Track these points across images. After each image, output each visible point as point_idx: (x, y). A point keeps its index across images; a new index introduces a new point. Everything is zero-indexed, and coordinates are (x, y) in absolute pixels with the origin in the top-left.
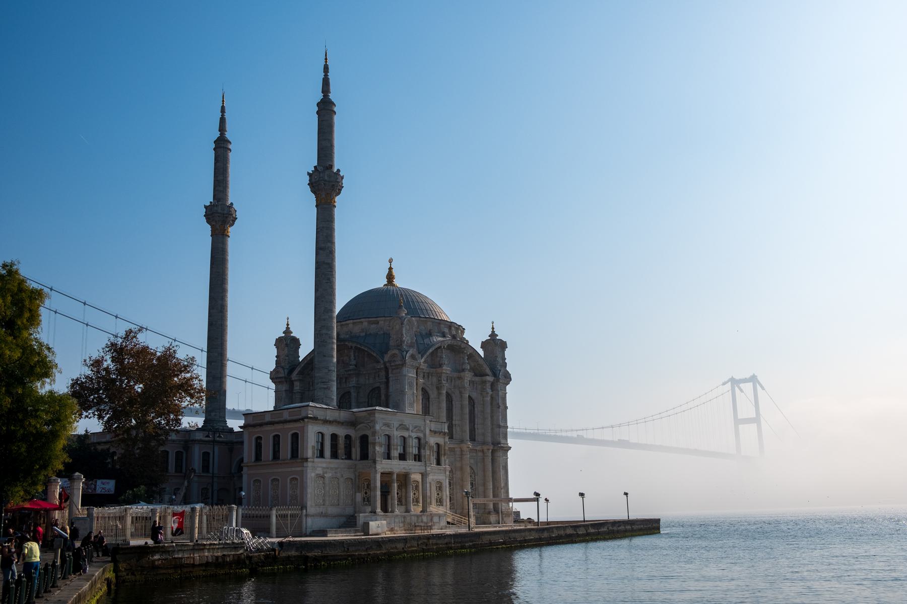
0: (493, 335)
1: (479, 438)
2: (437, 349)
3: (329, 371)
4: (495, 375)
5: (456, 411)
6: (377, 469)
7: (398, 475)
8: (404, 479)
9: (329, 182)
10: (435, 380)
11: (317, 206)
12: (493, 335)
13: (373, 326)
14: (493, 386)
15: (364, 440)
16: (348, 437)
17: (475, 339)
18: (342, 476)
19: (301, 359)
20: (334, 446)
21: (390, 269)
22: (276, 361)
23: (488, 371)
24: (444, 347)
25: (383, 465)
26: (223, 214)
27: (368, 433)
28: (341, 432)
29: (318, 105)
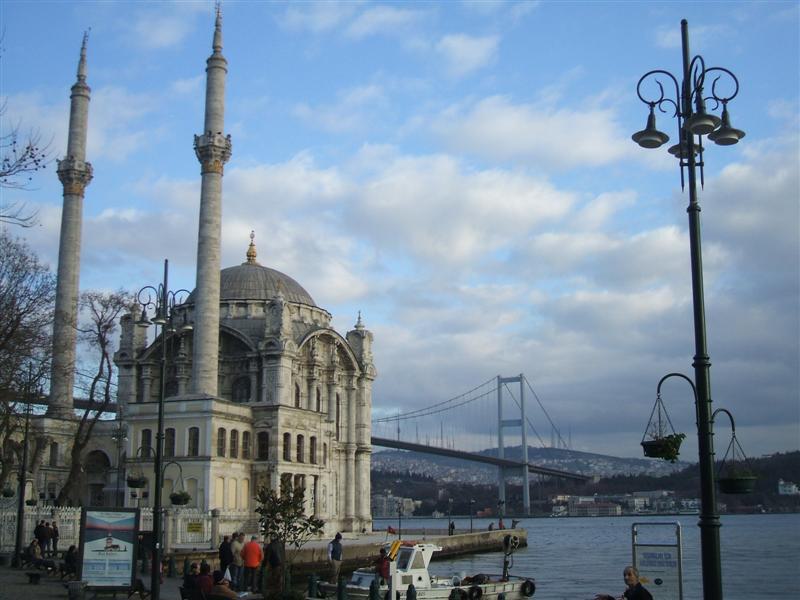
1: (343, 439)
4: (361, 368)
11: (202, 174)
13: (242, 309)
14: (359, 379)
20: (234, 443)
21: (252, 245)
25: (283, 468)
26: (80, 172)
27: (268, 430)
28: (242, 428)
29: (208, 62)
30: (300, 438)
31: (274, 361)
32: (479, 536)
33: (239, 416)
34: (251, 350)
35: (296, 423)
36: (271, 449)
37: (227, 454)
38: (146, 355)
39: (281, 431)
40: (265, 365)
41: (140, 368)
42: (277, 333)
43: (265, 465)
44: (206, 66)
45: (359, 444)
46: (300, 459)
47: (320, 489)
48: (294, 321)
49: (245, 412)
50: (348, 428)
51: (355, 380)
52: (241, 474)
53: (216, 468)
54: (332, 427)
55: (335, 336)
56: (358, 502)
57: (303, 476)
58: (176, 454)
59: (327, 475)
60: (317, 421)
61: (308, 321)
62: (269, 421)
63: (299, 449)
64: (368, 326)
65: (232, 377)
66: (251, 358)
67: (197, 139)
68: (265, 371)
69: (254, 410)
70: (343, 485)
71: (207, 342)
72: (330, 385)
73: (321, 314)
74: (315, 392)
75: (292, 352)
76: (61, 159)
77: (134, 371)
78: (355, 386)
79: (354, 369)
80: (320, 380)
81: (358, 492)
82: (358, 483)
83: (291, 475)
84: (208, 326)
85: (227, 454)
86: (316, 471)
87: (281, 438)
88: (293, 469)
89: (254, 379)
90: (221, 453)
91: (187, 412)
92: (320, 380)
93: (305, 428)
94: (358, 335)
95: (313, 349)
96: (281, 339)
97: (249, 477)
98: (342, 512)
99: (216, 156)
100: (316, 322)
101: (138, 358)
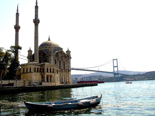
0: (68, 50)
1: (65, 69)
4: (68, 57)
5: (61, 64)
8: (51, 76)
10: (57, 58)
12: (68, 50)
15: (43, 69)
16: (40, 68)
17: (65, 50)
23: (67, 56)
25: (47, 74)
28: (39, 67)
30: (50, 69)
64: (70, 50)
77: (30, 59)
87: (46, 69)
88: (49, 74)
94: (68, 52)
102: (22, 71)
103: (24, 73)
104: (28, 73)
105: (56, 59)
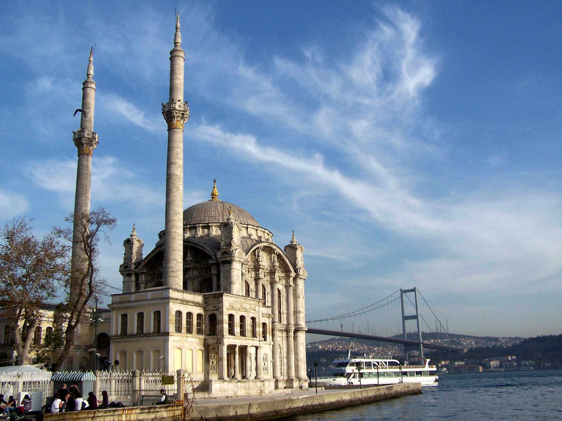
2: (255, 250)
3: (178, 262)
4: (296, 271)
5: (268, 298)
6: (224, 343)
7: (239, 346)
8: (243, 350)
9: (180, 111)
13: (206, 230)
14: (295, 279)
16: (199, 316)
18: (195, 348)
19: (144, 257)
20: (189, 323)
22: (124, 258)
24: (261, 248)
25: (228, 340)
26: (89, 138)
27: (216, 312)
30: (242, 318)
31: (228, 265)
32: (384, 389)
33: (193, 302)
34: (212, 258)
35: (238, 307)
36: (219, 326)
37: (184, 330)
38: (141, 266)
39: (226, 313)
40: (222, 268)
41: (137, 275)
42: (230, 245)
43: (214, 338)
44: (170, 56)
45: (296, 324)
46: (243, 333)
47: (260, 357)
48: (243, 237)
49: (199, 298)
50: (288, 314)
51: (291, 279)
52: (195, 346)
53: (174, 341)
54: (269, 311)
55: (274, 247)
56: (297, 367)
57: (246, 347)
58: (145, 332)
59: (268, 346)
60: (256, 305)
61: (254, 237)
62: (216, 306)
63: (242, 326)
65: (200, 279)
66: (212, 264)
67: (164, 106)
68: (222, 273)
69: (205, 298)
70: (285, 355)
71: (174, 250)
72: (273, 283)
73: (264, 232)
74: (260, 287)
75: (242, 258)
76: (76, 131)
77: (133, 278)
78: (292, 283)
79: (290, 271)
80: (265, 280)
81: (297, 359)
82: (296, 353)
83: (235, 346)
84: (173, 238)
85: (184, 330)
86: (256, 343)
87: (226, 318)
88: (238, 341)
89: (215, 279)
90: (179, 329)
91: (152, 299)
92: (265, 280)
93: (246, 310)
95: (258, 256)
96: (232, 248)
97: (203, 349)
98: (286, 374)
99: (177, 117)
100: (260, 237)
101: (136, 268)
102: (115, 329)
103: (124, 333)
104: (148, 335)
105: (250, 277)
